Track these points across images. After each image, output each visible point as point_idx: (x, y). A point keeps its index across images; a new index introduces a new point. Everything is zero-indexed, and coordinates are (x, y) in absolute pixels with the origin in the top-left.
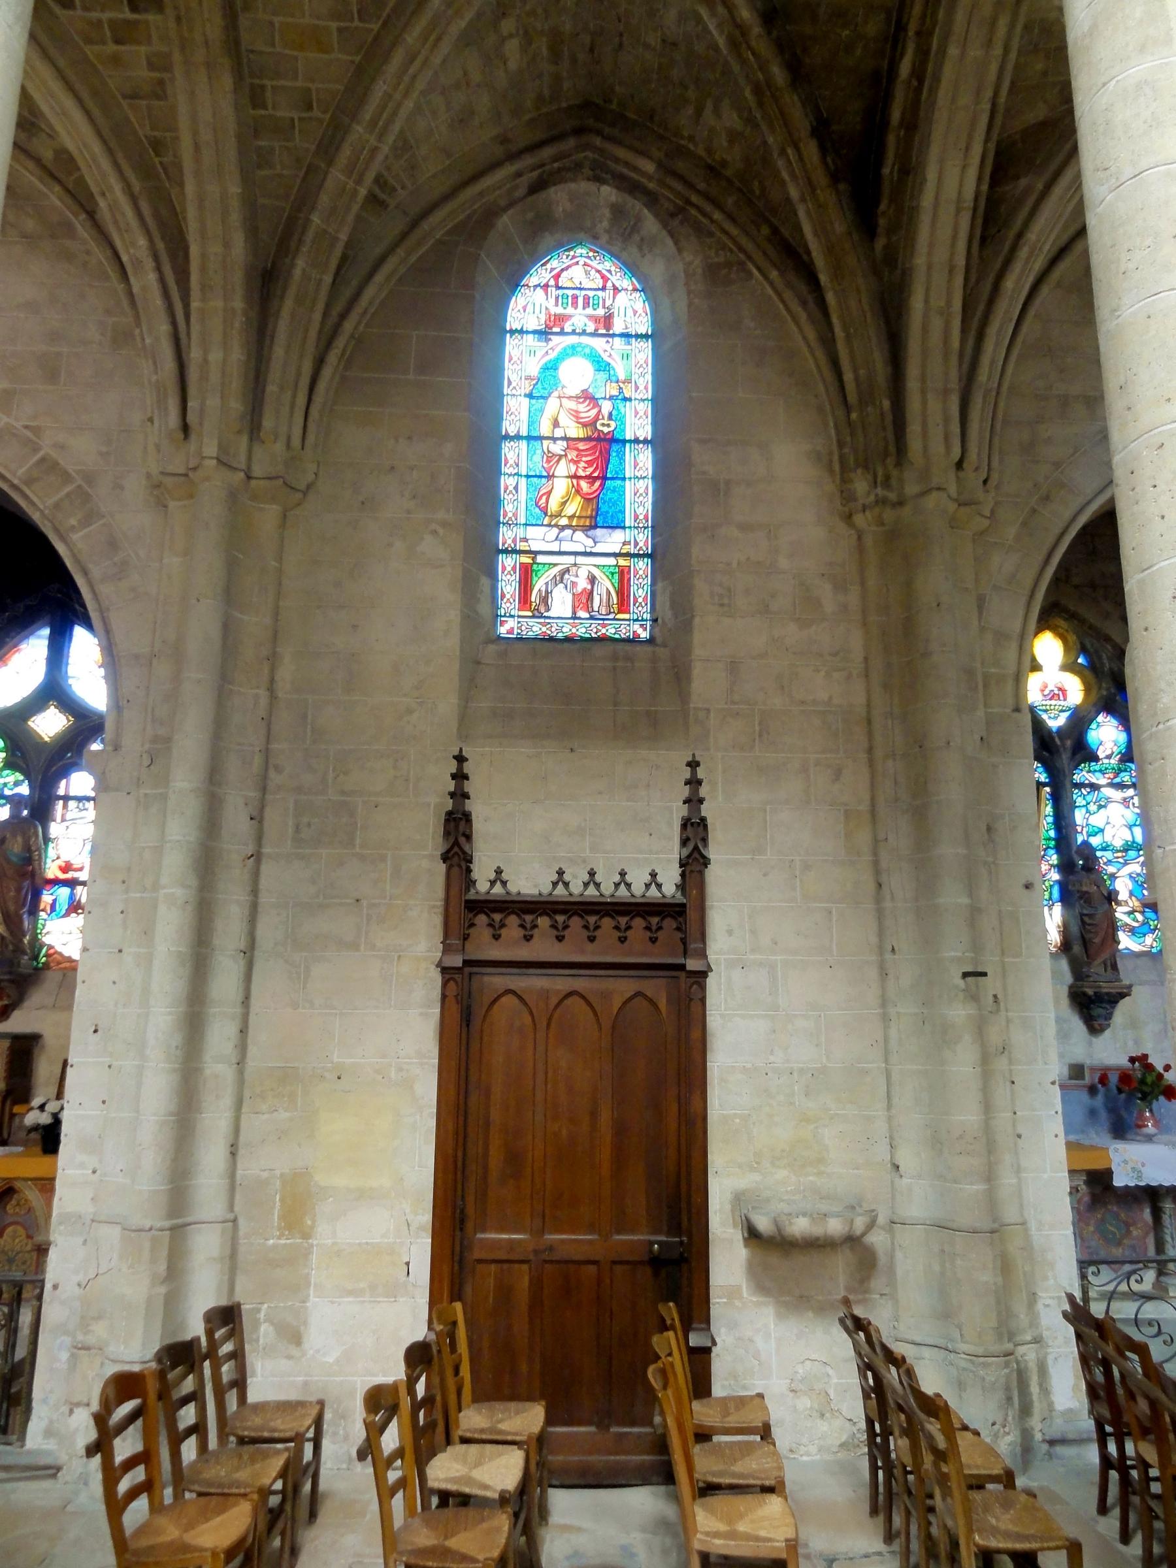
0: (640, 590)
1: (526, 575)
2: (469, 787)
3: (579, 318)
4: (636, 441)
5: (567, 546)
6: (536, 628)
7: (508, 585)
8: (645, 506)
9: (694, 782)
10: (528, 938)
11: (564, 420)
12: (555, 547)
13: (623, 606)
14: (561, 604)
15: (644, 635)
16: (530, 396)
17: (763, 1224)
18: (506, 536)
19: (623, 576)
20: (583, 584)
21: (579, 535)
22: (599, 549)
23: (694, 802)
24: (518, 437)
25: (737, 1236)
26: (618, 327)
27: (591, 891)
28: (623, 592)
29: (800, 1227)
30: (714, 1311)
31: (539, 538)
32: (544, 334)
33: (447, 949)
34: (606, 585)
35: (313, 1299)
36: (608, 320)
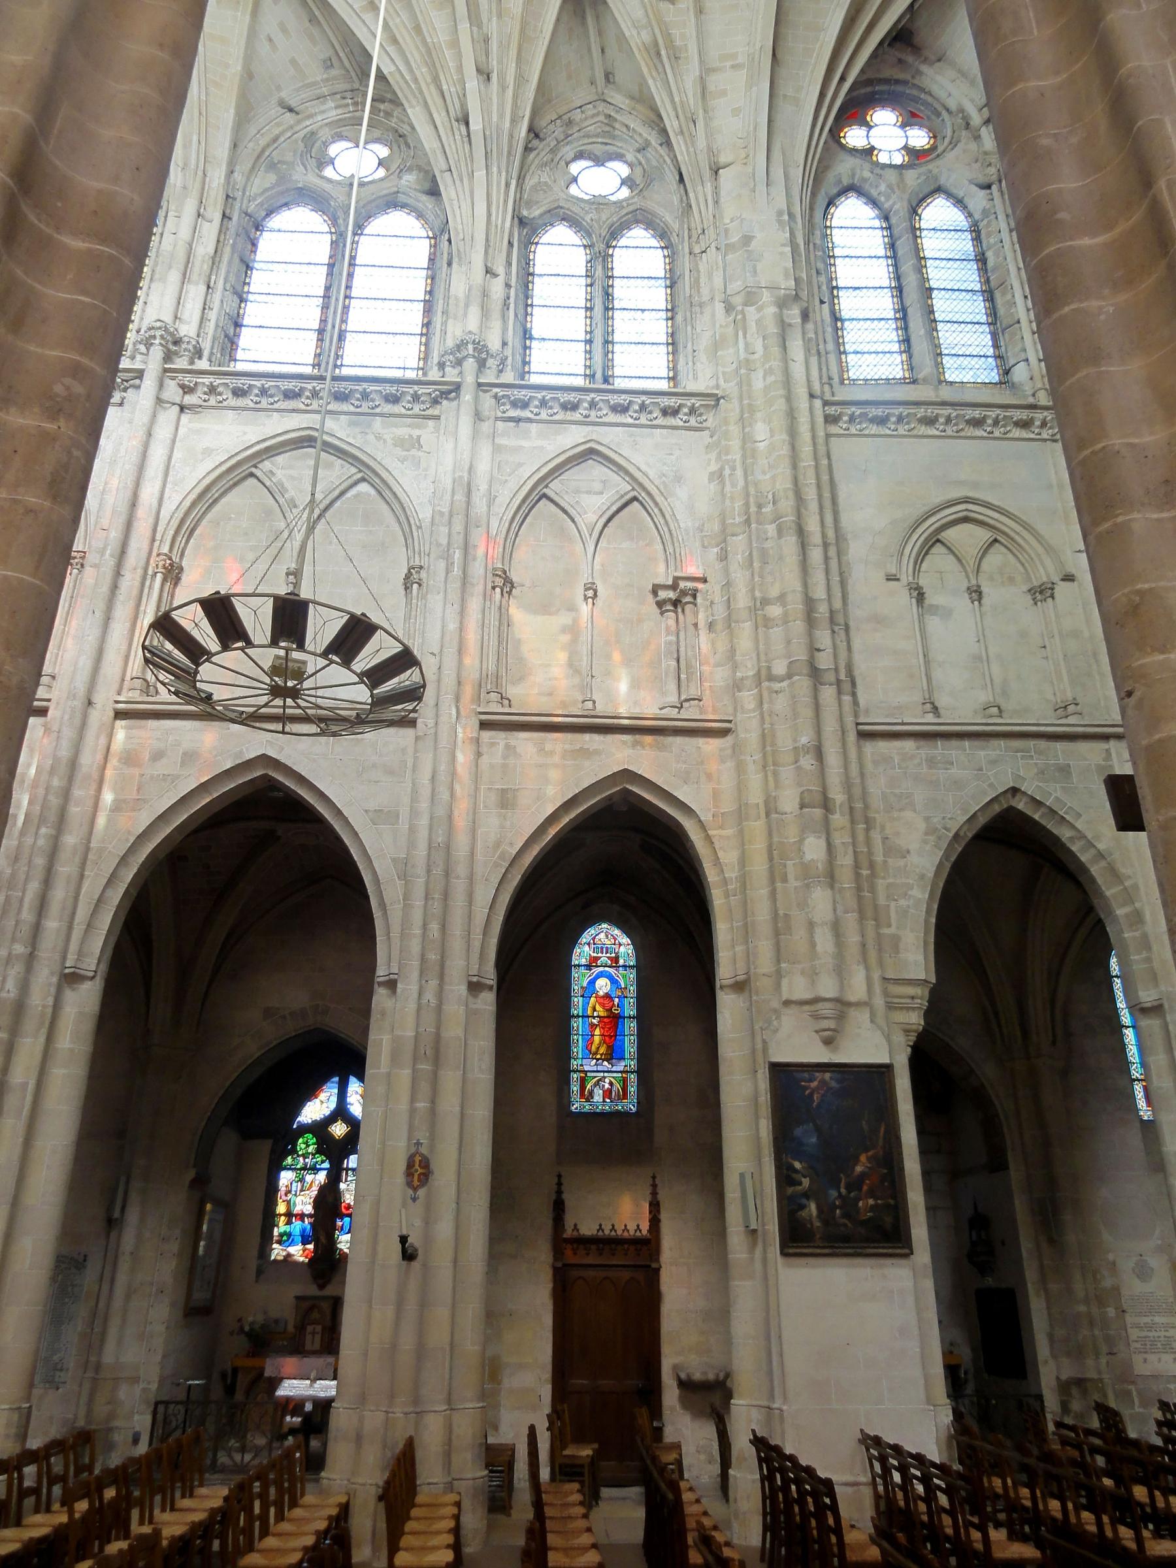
0: (632, 1090)
1: (583, 1082)
2: (563, 1188)
3: (604, 959)
4: (630, 1017)
5: (600, 1068)
6: (588, 1108)
7: (575, 1088)
8: (634, 1050)
9: (654, 1186)
10: (588, 1254)
11: (598, 1007)
12: (595, 1068)
13: (625, 1096)
14: (598, 1096)
15: (634, 1109)
16: (582, 996)
17: (683, 1376)
18: (574, 1064)
19: (625, 1080)
20: (607, 1086)
21: (606, 1063)
22: (614, 1069)
23: (654, 1194)
24: (578, 1016)
25: (675, 1384)
26: (621, 962)
27: (613, 1233)
28: (625, 1089)
29: (697, 1376)
30: (664, 1417)
31: (590, 1065)
32: (589, 967)
33: (556, 1259)
34: (617, 1086)
35: (502, 1411)
36: (616, 960)
